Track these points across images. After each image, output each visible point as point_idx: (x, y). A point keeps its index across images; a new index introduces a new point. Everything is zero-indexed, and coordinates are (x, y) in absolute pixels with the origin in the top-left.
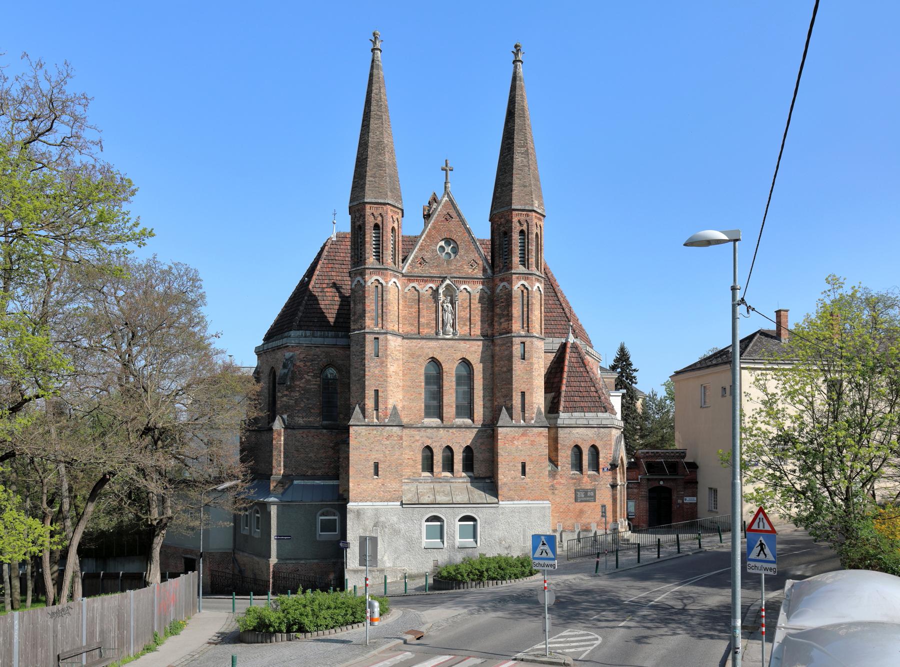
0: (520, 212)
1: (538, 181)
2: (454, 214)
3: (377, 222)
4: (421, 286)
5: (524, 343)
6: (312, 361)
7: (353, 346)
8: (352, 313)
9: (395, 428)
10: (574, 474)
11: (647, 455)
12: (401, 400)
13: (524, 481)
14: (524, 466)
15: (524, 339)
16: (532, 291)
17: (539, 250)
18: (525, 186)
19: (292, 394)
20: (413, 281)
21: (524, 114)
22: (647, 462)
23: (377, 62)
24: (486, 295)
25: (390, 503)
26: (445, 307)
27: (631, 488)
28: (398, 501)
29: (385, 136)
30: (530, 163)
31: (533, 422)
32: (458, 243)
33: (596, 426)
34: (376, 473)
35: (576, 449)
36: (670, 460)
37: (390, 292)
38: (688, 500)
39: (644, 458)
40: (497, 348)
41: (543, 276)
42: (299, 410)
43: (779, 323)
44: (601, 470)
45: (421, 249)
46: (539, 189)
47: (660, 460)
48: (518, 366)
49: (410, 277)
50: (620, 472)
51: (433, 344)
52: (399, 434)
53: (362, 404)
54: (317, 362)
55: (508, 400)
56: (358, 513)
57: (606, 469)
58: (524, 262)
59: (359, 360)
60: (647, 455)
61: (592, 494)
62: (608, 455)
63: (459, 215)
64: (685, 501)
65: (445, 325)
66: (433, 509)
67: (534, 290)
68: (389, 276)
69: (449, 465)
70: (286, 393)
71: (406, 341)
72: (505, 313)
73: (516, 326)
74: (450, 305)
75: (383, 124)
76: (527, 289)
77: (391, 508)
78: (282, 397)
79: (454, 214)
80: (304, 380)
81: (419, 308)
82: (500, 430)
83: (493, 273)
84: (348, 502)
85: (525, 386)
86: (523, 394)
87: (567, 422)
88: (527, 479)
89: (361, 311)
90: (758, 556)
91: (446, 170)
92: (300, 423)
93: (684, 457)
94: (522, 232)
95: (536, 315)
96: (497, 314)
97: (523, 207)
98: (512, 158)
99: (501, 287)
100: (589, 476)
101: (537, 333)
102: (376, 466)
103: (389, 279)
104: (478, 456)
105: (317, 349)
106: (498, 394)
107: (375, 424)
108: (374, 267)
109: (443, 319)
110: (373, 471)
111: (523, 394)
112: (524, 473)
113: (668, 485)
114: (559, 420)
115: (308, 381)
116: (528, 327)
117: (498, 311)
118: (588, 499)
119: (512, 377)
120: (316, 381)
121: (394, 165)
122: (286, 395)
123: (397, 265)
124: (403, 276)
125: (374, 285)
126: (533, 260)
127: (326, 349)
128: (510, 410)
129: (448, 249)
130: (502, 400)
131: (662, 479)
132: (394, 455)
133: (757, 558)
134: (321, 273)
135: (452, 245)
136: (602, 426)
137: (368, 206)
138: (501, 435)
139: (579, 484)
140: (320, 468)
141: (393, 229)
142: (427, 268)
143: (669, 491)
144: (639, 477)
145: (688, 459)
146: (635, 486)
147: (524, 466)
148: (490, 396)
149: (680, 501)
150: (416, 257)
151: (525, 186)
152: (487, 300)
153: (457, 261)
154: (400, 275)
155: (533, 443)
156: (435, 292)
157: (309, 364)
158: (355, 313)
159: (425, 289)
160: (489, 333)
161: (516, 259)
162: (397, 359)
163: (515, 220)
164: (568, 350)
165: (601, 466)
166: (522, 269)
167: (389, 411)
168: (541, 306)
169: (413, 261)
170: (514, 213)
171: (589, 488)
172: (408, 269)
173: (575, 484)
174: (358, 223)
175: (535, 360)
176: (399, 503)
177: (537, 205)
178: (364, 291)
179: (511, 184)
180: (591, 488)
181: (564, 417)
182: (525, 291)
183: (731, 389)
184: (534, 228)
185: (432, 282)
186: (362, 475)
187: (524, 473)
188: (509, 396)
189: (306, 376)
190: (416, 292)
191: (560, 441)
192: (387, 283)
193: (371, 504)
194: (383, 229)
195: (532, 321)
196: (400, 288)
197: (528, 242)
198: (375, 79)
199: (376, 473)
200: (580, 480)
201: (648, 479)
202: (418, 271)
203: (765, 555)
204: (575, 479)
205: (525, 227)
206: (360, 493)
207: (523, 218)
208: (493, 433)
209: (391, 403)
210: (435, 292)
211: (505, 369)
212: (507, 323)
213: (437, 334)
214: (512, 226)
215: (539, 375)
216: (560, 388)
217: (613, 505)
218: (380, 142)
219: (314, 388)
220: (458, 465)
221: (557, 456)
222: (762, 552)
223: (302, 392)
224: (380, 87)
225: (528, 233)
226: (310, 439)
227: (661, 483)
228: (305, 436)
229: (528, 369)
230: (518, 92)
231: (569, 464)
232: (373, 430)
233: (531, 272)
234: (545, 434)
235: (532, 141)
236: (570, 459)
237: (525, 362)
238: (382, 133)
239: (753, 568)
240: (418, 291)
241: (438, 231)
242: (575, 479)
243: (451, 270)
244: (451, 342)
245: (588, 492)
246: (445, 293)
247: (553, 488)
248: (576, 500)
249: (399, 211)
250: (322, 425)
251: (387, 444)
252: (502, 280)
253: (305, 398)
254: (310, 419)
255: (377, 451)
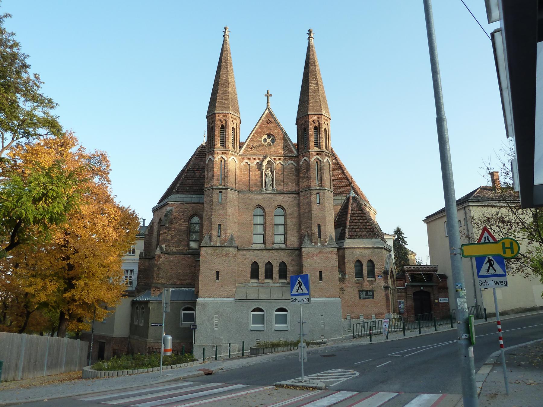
0: (314, 116)
1: (325, 99)
2: (272, 120)
3: (223, 124)
4: (251, 162)
5: (318, 193)
6: (184, 212)
7: (205, 197)
8: (206, 178)
9: (231, 249)
10: (357, 280)
11: (410, 269)
12: (236, 231)
13: (321, 284)
14: (321, 273)
15: (318, 191)
16: (323, 161)
17: (327, 138)
18: (316, 102)
19: (170, 232)
20: (246, 159)
21: (315, 64)
22: (410, 274)
23: (226, 41)
24: (293, 167)
25: (226, 299)
26: (267, 174)
27: (400, 292)
28: (232, 297)
29: (229, 78)
30: (319, 89)
31: (326, 244)
32: (275, 136)
33: (371, 247)
34: (218, 278)
35: (358, 264)
36: (426, 273)
37: (230, 164)
38: (442, 300)
39: (408, 271)
40: (301, 198)
41: (331, 154)
42: (173, 243)
43: (493, 181)
44: (377, 277)
45: (252, 140)
46: (326, 104)
47: (419, 273)
48: (315, 208)
49: (244, 157)
50: (391, 280)
51: (259, 196)
52: (234, 252)
53: (209, 233)
54: (186, 213)
55: (309, 230)
56: (204, 305)
57: (380, 276)
58: (318, 144)
59: (209, 206)
60: (410, 269)
61: (371, 293)
62: (381, 267)
63: (276, 120)
64: (440, 301)
65: (267, 184)
66: (257, 303)
67: (325, 161)
68: (229, 155)
69: (269, 275)
70: (165, 231)
71: (241, 195)
72: (306, 175)
73: (314, 183)
74: (270, 173)
75: (228, 72)
76: (320, 160)
77: (227, 302)
78: (163, 234)
79: (272, 120)
80: (178, 224)
81: (250, 175)
82: (304, 250)
83: (298, 153)
84: (198, 298)
85: (320, 221)
86: (319, 226)
87: (351, 244)
88: (323, 283)
89: (211, 176)
90: (488, 271)
91: (268, 96)
92: (174, 251)
93: (436, 271)
94: (315, 128)
95: (326, 176)
96: (301, 177)
97: (316, 113)
98: (308, 87)
99: (303, 161)
100: (368, 281)
101: (328, 188)
102: (218, 273)
103: (229, 157)
104: (290, 268)
105: (187, 205)
106: (302, 227)
107: (218, 246)
108: (220, 149)
109: (265, 182)
110: (215, 277)
111: (319, 226)
112: (321, 278)
113: (427, 290)
114: (345, 243)
115: (180, 224)
116: (321, 183)
117: (301, 175)
118: (368, 297)
119: (311, 215)
120: (185, 225)
121: (235, 93)
122: (165, 233)
123: (235, 149)
124: (240, 156)
125: (220, 160)
126: (323, 143)
127: (193, 205)
128: (310, 237)
129: (269, 140)
130: (305, 230)
131: (422, 286)
132: (230, 267)
133: (487, 274)
134: (194, 163)
135: (271, 138)
136: (375, 247)
137: (217, 115)
138: (305, 253)
139: (361, 286)
140: (185, 280)
141: (233, 128)
142: (255, 151)
143: (428, 294)
144: (406, 284)
145: (439, 272)
146: (403, 291)
147: (321, 273)
148: (297, 229)
149: (436, 301)
150: (248, 145)
151: (316, 102)
152: (295, 170)
153: (275, 146)
154: (237, 155)
155: (327, 258)
156: (260, 166)
157: (181, 214)
158: (207, 177)
159: (254, 164)
160: (296, 189)
161: (312, 143)
162: (235, 206)
163: (311, 120)
164: (351, 201)
165: (376, 274)
166: (316, 149)
167: (228, 238)
168: (330, 172)
169: (246, 148)
170: (309, 116)
171: (368, 289)
172: (243, 152)
173: (358, 286)
174: (211, 126)
175: (327, 205)
176: (233, 299)
177: (325, 112)
178: (213, 164)
179: (308, 100)
180: (370, 289)
181: (348, 242)
182: (319, 162)
183: (464, 221)
184: (323, 125)
185: (258, 159)
186: (208, 280)
187: (321, 278)
188: (310, 227)
189: (179, 221)
190: (248, 166)
191: (346, 257)
192: (228, 158)
193: (213, 299)
194: (226, 127)
195: (324, 180)
196: (237, 163)
197: (320, 133)
198: (224, 49)
199: (218, 278)
200: (361, 284)
201: (412, 286)
202: (250, 152)
203: (495, 270)
204: (358, 283)
205: (317, 124)
206: (206, 292)
207: (315, 119)
208: (300, 253)
209: (229, 232)
210: (260, 166)
211: (306, 211)
212: (307, 182)
213: (261, 190)
214: (309, 124)
215: (330, 214)
216: (346, 223)
217: (386, 301)
218: (226, 81)
219: (184, 229)
220: (276, 275)
221: (345, 267)
222: (491, 268)
223: (176, 231)
224: (227, 53)
225: (319, 128)
226: (180, 260)
227: (422, 288)
228: (176, 259)
229: (322, 210)
230: (311, 53)
231: (353, 273)
232: (216, 250)
233: (322, 150)
234: (334, 252)
235: (321, 78)
236: (354, 270)
237: (320, 206)
238: (227, 76)
239: (484, 284)
240: (249, 165)
241: (262, 130)
242: (358, 283)
243: (271, 152)
244: (270, 196)
245: (368, 292)
246: (267, 166)
247: (342, 289)
248: (360, 298)
249: (238, 118)
250: (188, 252)
251: (226, 259)
252: (303, 156)
253: (178, 235)
254: (181, 248)
255: (219, 263)
